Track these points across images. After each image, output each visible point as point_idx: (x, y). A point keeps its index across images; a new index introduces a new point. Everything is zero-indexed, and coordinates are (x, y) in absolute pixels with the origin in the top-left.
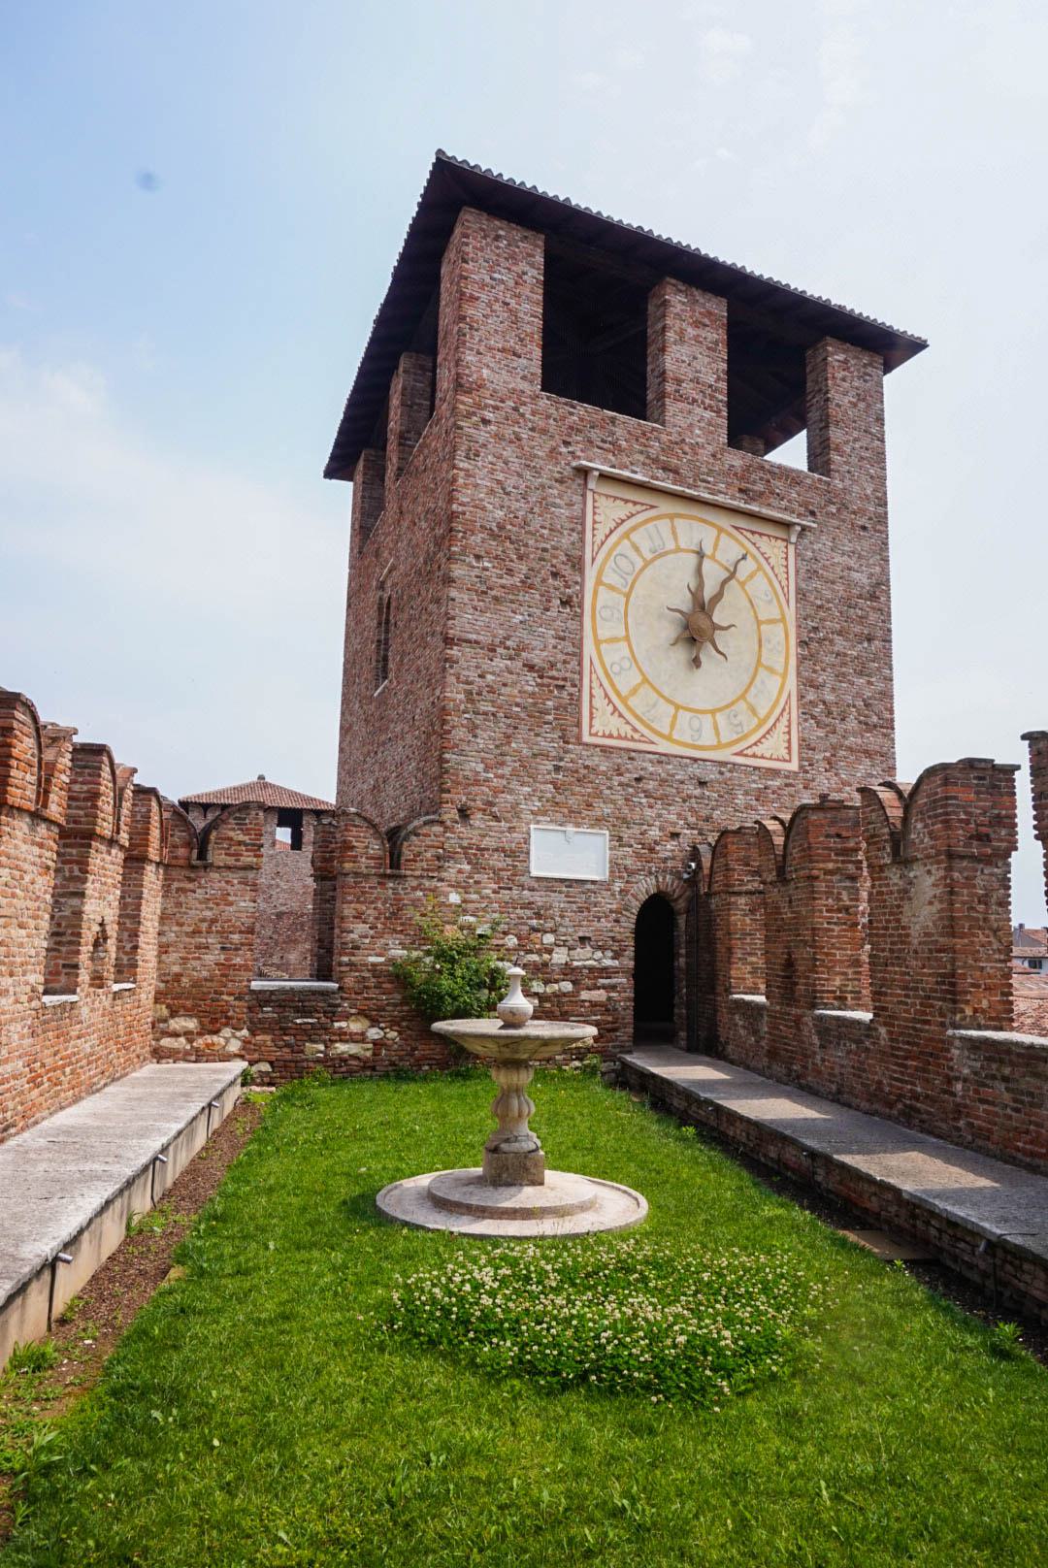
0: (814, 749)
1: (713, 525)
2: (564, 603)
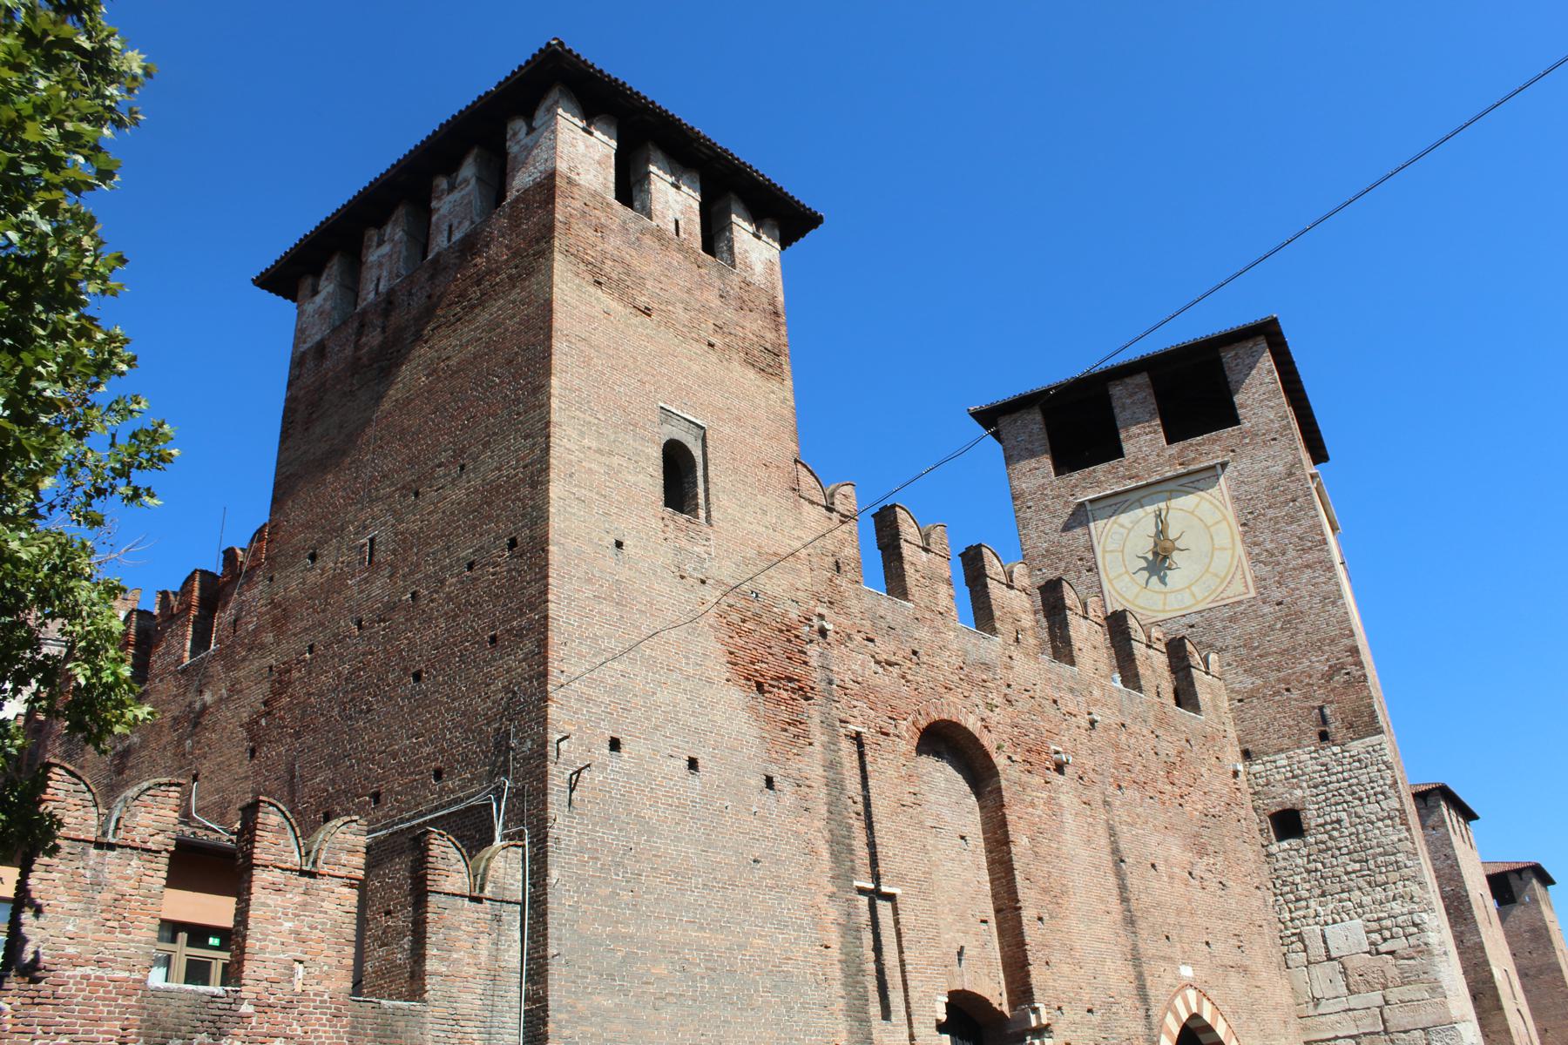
0: (1265, 580)
1: (1166, 491)
2: (1088, 571)
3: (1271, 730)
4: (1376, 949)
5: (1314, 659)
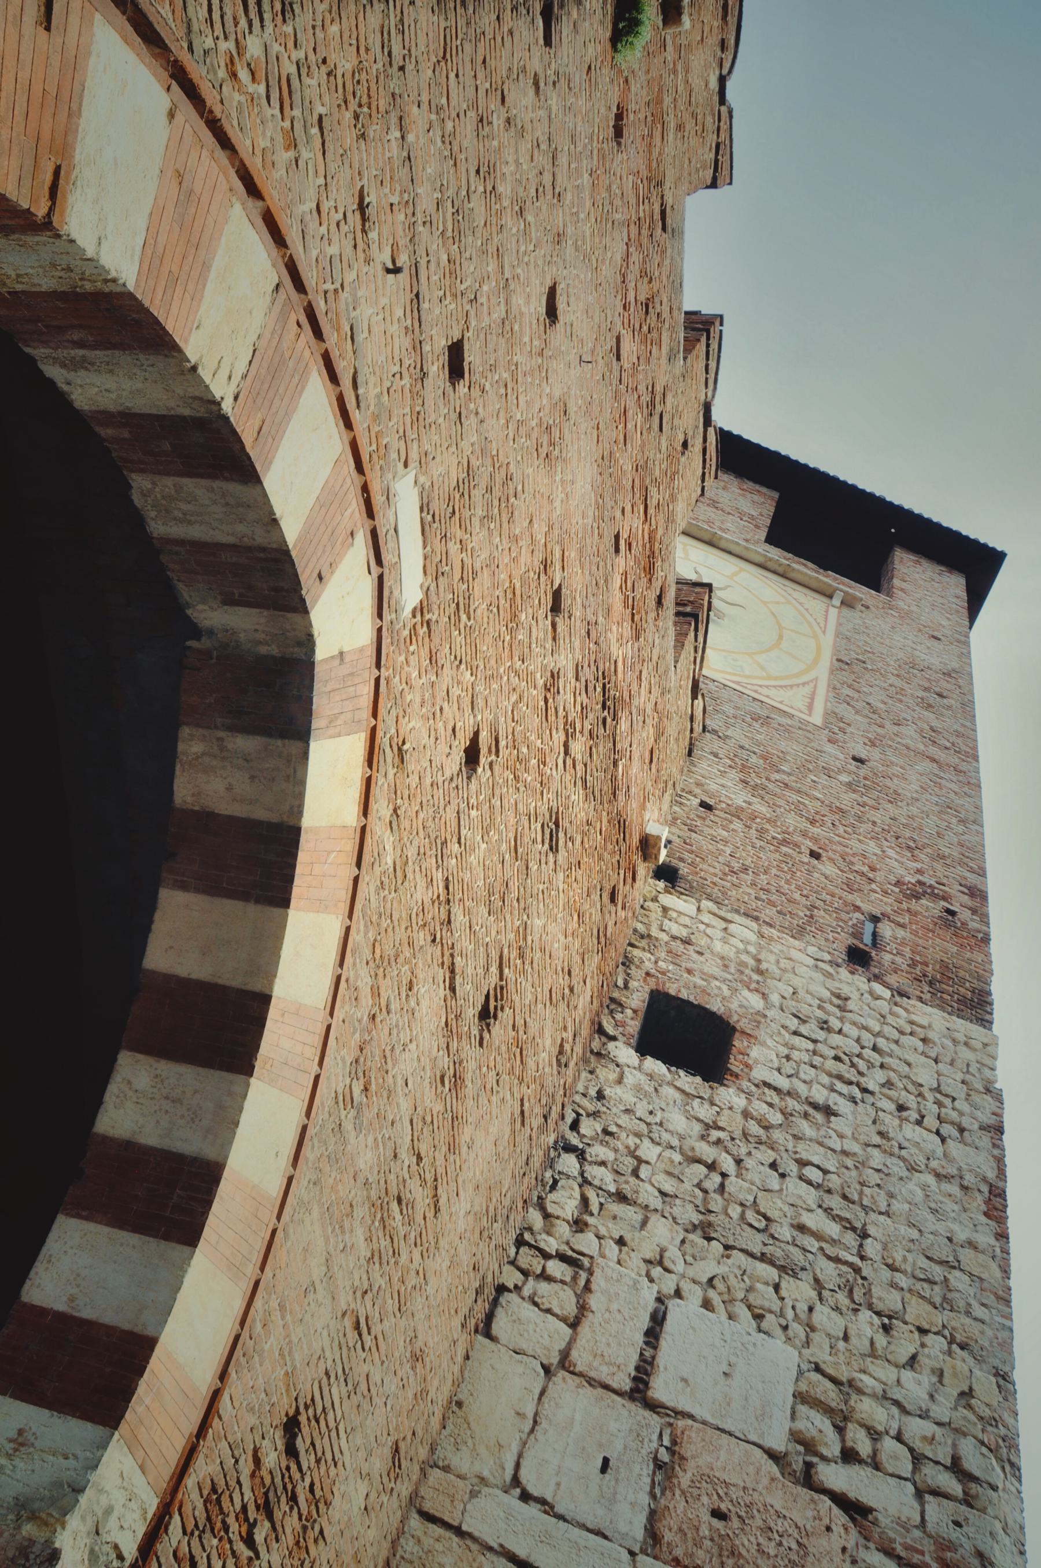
3: (749, 878)
4: (809, 1466)
5: (891, 852)
